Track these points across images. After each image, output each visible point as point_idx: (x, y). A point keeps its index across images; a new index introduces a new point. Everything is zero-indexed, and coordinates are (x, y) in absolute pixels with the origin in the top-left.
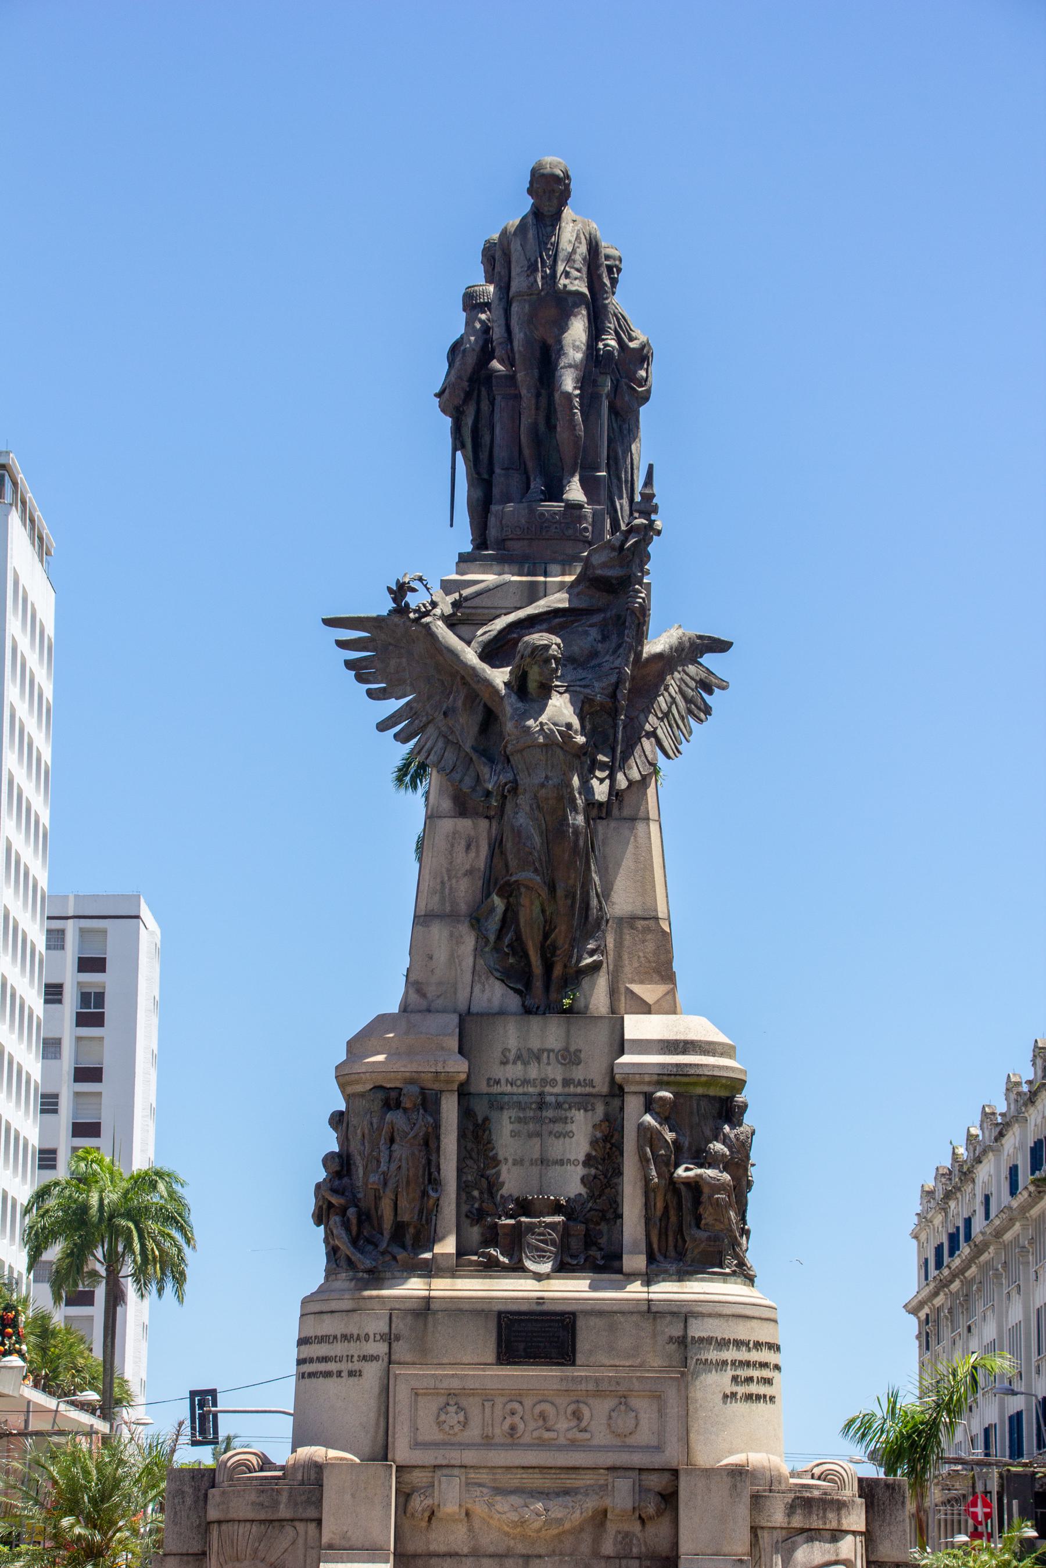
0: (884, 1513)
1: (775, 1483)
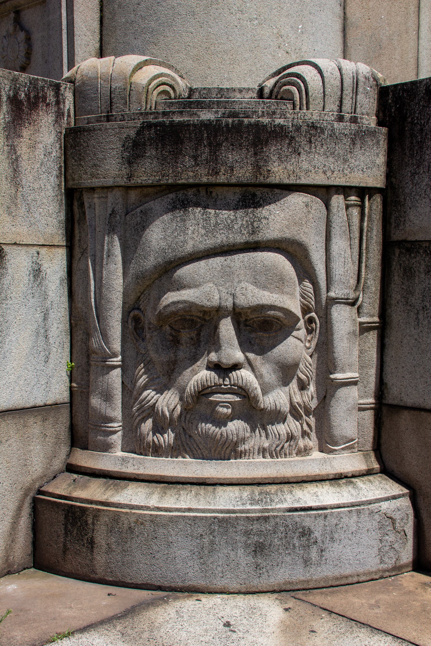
0: (421, 148)
1: (118, 105)
